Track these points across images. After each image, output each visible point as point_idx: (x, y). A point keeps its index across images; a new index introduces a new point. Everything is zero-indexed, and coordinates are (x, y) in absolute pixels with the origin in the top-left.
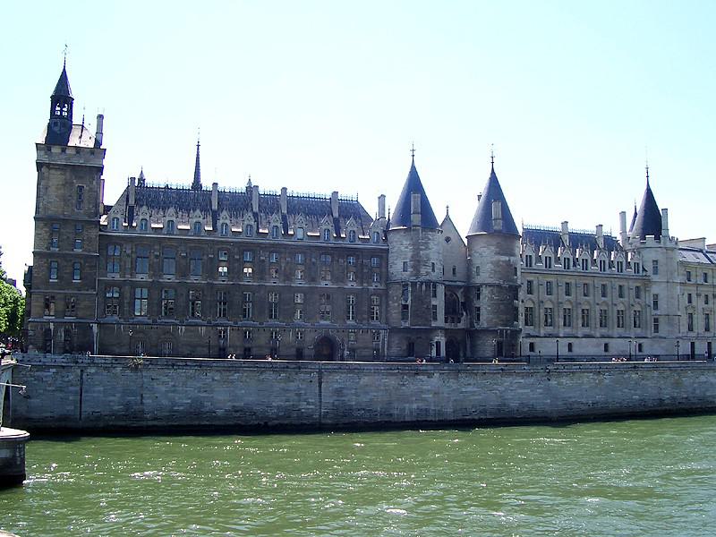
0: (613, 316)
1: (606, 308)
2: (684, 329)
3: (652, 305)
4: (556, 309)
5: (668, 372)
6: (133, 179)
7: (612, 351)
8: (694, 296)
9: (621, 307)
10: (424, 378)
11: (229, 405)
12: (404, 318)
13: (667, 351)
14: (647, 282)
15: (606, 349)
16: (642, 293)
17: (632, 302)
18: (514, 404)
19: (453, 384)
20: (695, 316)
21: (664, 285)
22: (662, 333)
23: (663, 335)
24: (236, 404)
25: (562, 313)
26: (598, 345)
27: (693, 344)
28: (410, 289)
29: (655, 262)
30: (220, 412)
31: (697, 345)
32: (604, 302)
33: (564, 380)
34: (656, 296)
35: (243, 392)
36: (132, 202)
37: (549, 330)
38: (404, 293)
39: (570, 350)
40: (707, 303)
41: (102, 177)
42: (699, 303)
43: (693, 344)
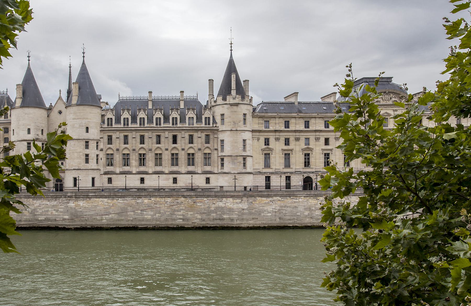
0: (183, 157)
1: (175, 152)
3: (219, 149)
4: (131, 155)
5: (183, 199)
8: (272, 140)
9: (191, 151)
13: (229, 183)
14: (216, 131)
16: (211, 142)
17: (200, 147)
20: (272, 156)
21: (228, 133)
22: (226, 169)
23: (226, 171)
26: (168, 179)
29: (222, 115)
32: (175, 148)
33: (82, 203)
34: (222, 141)
37: (126, 169)
42: (277, 147)
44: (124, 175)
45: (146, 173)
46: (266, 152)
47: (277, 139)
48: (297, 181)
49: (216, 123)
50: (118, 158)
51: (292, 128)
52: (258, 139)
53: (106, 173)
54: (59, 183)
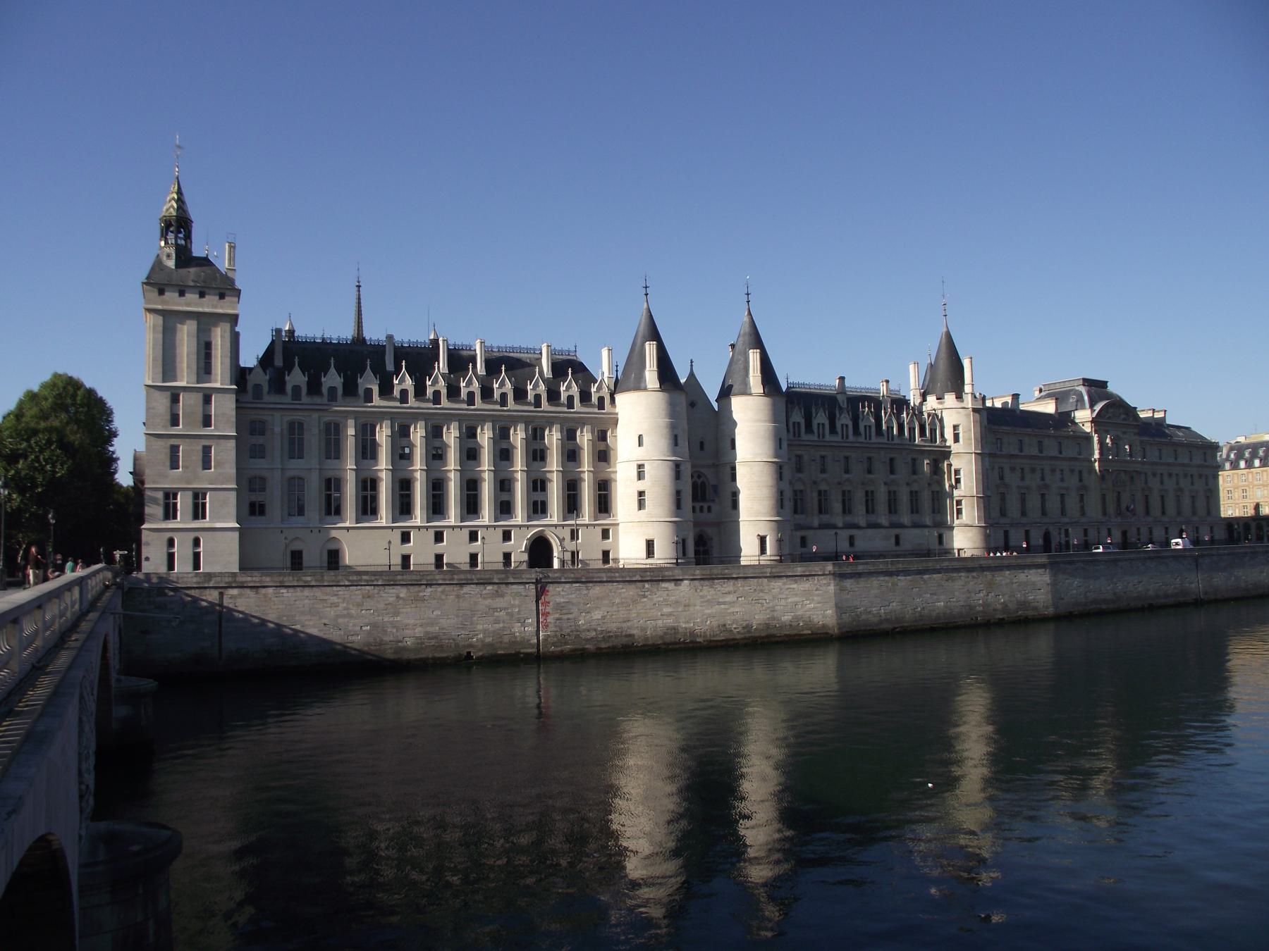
0: (904, 499)
2: (995, 513)
6: (278, 331)
7: (906, 545)
8: (1007, 471)
10: (671, 586)
11: (419, 632)
12: (641, 505)
14: (946, 454)
15: (897, 538)
18: (786, 618)
19: (707, 591)
24: (429, 629)
25: (840, 497)
27: (1006, 533)
28: (646, 469)
30: (409, 642)
31: (1012, 533)
34: (957, 472)
35: (437, 613)
36: (279, 362)
38: (640, 476)
39: (852, 544)
40: (1023, 478)
41: (237, 329)
42: (1013, 479)
43: (1006, 533)
44: (833, 532)
45: (857, 527)
46: (1001, 490)
47: (1013, 469)
48: (1038, 540)
49: (945, 441)
50: (812, 499)
51: (1026, 452)
52: (993, 469)
53: (799, 527)
54: (702, 549)
